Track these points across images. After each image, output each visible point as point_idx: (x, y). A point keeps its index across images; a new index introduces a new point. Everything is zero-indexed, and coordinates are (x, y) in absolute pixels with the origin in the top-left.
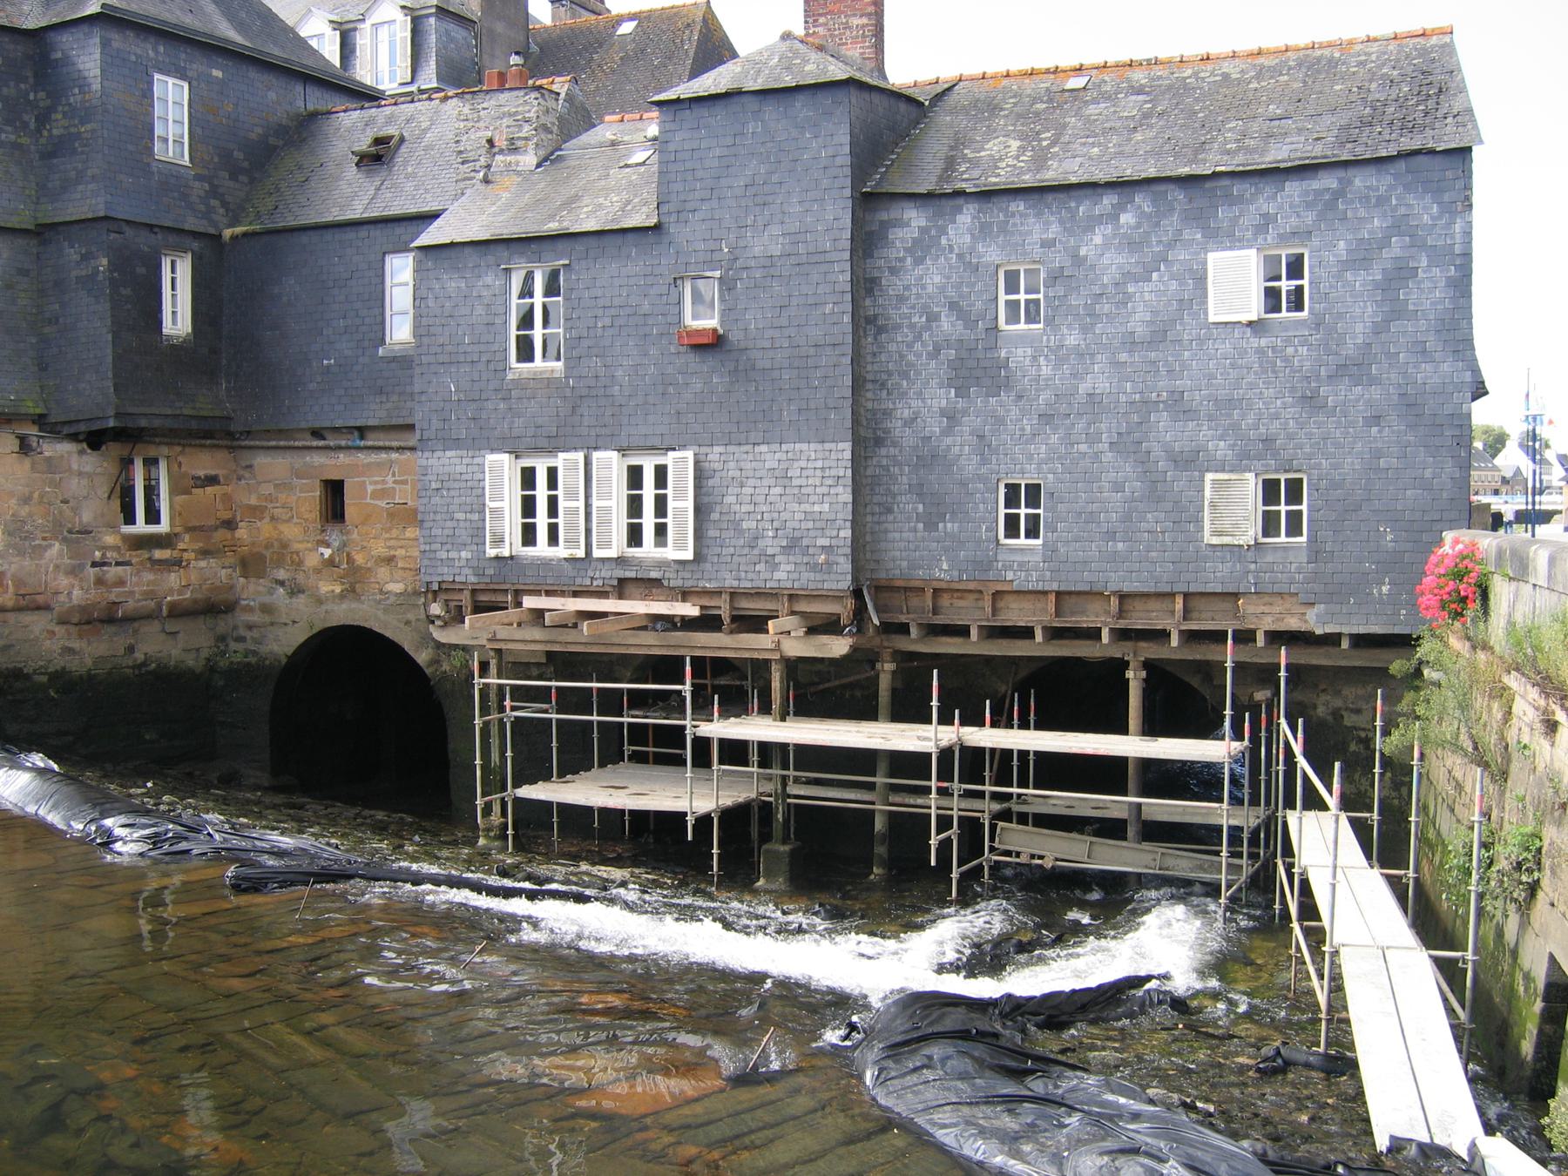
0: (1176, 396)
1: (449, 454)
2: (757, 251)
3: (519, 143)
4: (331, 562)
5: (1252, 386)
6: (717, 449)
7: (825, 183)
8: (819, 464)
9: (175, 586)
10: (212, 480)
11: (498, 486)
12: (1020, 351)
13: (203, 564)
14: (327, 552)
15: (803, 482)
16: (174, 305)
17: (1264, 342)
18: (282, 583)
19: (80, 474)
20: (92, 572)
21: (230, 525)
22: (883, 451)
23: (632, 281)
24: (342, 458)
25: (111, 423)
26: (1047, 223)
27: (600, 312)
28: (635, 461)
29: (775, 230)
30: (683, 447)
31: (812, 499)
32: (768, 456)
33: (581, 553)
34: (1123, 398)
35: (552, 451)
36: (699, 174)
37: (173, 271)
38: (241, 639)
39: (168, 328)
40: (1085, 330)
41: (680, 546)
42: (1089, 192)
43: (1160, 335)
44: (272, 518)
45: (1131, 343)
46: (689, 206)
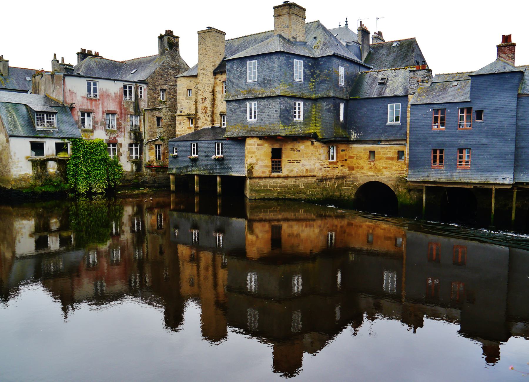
9: (337, 172)
25: (333, 139)
44: (357, 159)
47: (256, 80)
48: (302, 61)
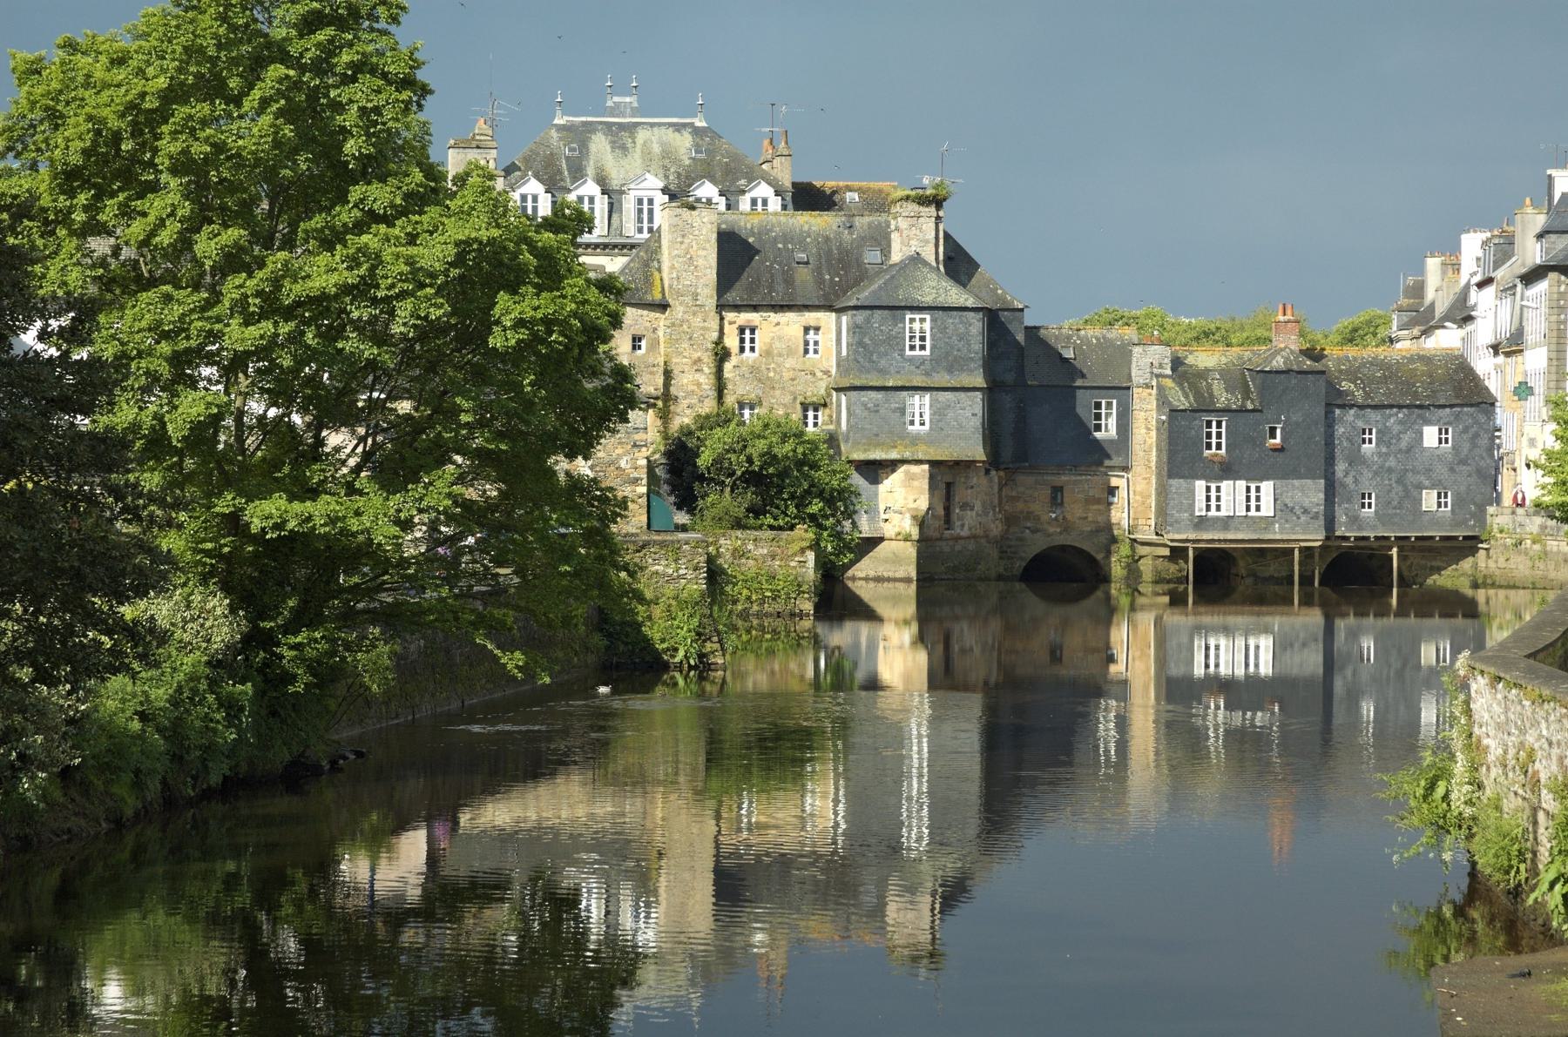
43: (1409, 450)
47: (927, 352)
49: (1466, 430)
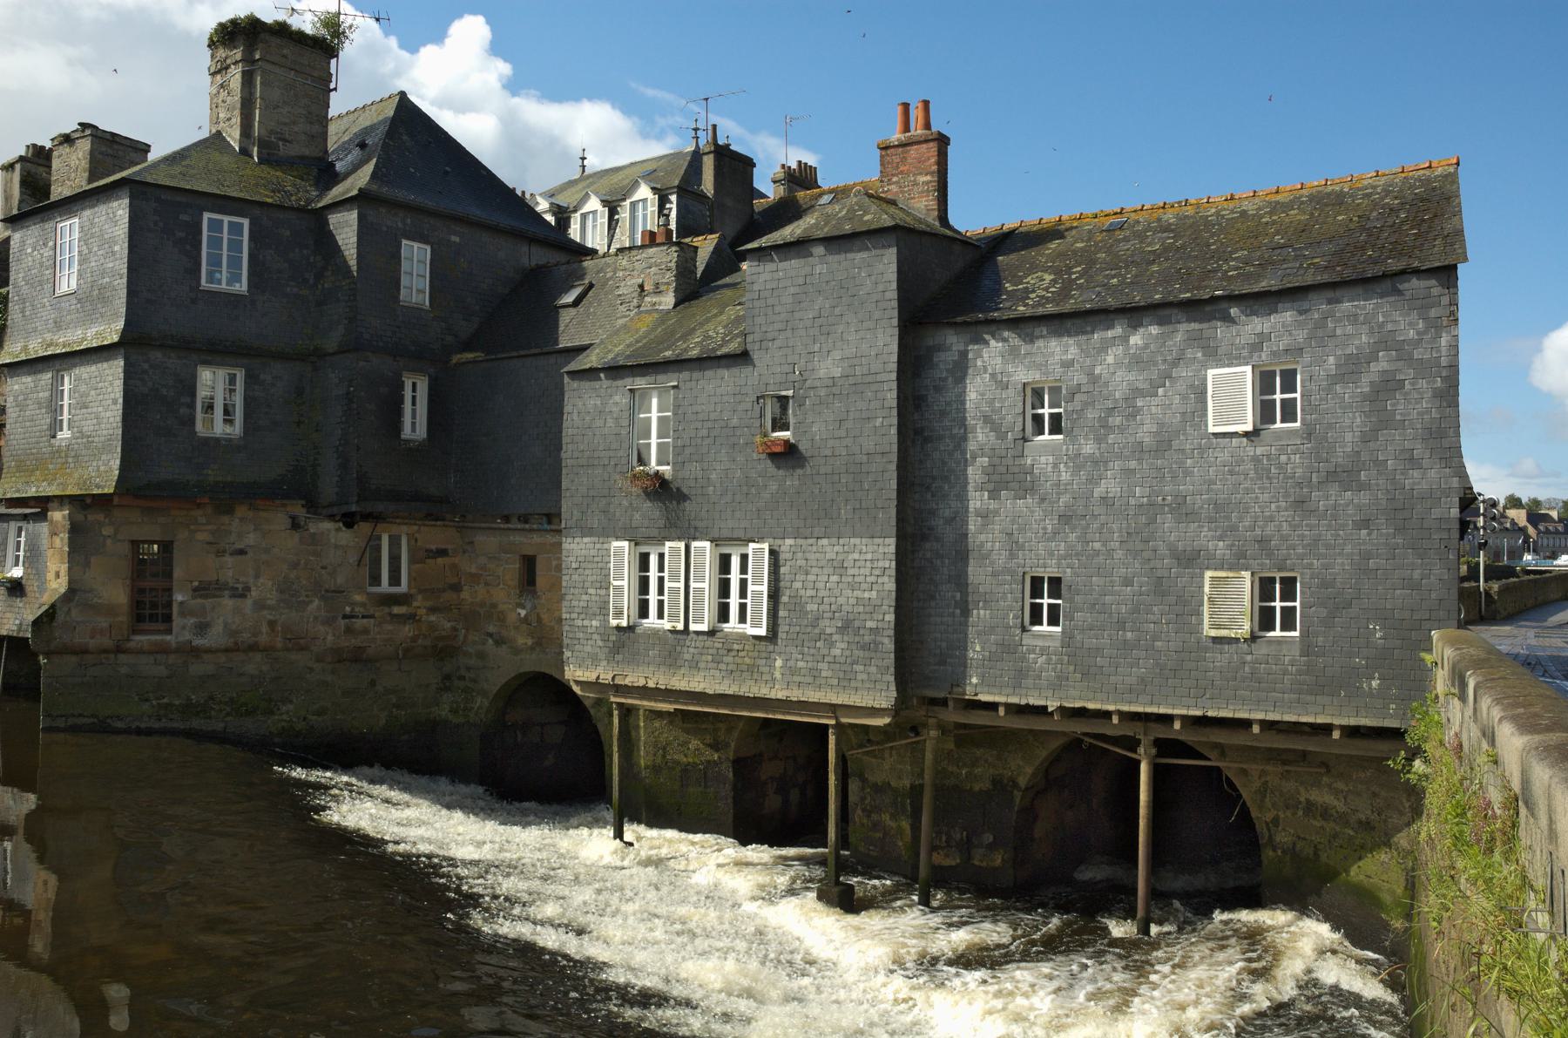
0: (1180, 500)
1: (586, 540)
2: (822, 373)
3: (662, 288)
4: (526, 620)
5: (1247, 491)
6: (789, 542)
7: (877, 315)
8: (869, 556)
10: (442, 553)
11: (619, 567)
12: (1043, 459)
13: (433, 618)
14: (523, 613)
15: (855, 571)
16: (414, 417)
17: (1259, 451)
18: (491, 635)
19: (336, 547)
20: (342, 623)
21: (456, 588)
22: (928, 545)
23: (725, 398)
24: (536, 539)
26: (1067, 346)
27: (699, 425)
28: (726, 550)
29: (837, 355)
30: (760, 540)
31: (864, 586)
32: (828, 549)
33: (680, 626)
34: (1132, 501)
35: (661, 541)
36: (777, 309)
37: (414, 390)
38: (462, 678)
39: (407, 432)
40: (1099, 440)
41: (755, 625)
42: (1103, 317)
43: (1163, 443)
45: (1139, 450)
46: (770, 336)
48: (246, 222)
49: (1351, 368)
